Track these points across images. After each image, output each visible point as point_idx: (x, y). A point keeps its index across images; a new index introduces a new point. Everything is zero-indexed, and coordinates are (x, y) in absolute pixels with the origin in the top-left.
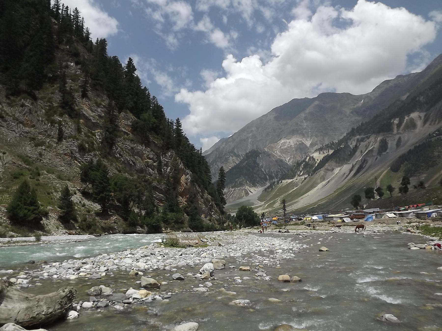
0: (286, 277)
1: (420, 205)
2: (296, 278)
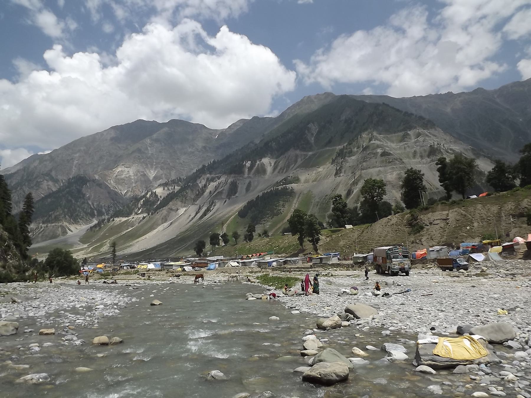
0: (104, 339)
1: (262, 254)
2: (117, 339)
